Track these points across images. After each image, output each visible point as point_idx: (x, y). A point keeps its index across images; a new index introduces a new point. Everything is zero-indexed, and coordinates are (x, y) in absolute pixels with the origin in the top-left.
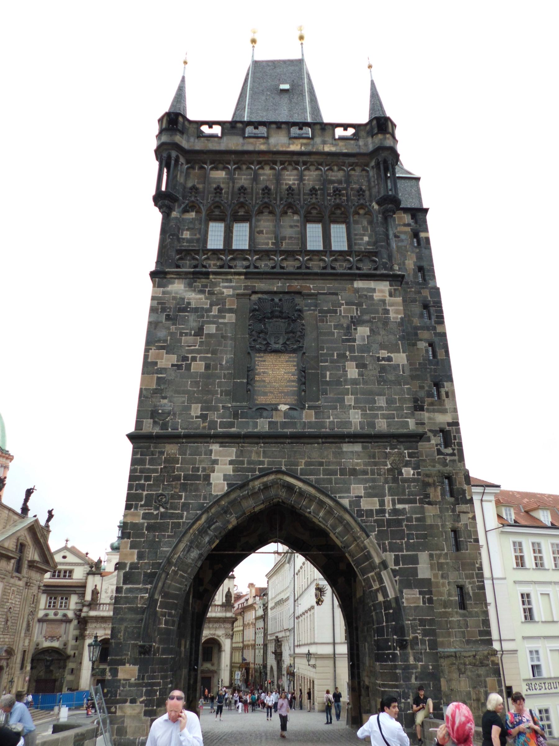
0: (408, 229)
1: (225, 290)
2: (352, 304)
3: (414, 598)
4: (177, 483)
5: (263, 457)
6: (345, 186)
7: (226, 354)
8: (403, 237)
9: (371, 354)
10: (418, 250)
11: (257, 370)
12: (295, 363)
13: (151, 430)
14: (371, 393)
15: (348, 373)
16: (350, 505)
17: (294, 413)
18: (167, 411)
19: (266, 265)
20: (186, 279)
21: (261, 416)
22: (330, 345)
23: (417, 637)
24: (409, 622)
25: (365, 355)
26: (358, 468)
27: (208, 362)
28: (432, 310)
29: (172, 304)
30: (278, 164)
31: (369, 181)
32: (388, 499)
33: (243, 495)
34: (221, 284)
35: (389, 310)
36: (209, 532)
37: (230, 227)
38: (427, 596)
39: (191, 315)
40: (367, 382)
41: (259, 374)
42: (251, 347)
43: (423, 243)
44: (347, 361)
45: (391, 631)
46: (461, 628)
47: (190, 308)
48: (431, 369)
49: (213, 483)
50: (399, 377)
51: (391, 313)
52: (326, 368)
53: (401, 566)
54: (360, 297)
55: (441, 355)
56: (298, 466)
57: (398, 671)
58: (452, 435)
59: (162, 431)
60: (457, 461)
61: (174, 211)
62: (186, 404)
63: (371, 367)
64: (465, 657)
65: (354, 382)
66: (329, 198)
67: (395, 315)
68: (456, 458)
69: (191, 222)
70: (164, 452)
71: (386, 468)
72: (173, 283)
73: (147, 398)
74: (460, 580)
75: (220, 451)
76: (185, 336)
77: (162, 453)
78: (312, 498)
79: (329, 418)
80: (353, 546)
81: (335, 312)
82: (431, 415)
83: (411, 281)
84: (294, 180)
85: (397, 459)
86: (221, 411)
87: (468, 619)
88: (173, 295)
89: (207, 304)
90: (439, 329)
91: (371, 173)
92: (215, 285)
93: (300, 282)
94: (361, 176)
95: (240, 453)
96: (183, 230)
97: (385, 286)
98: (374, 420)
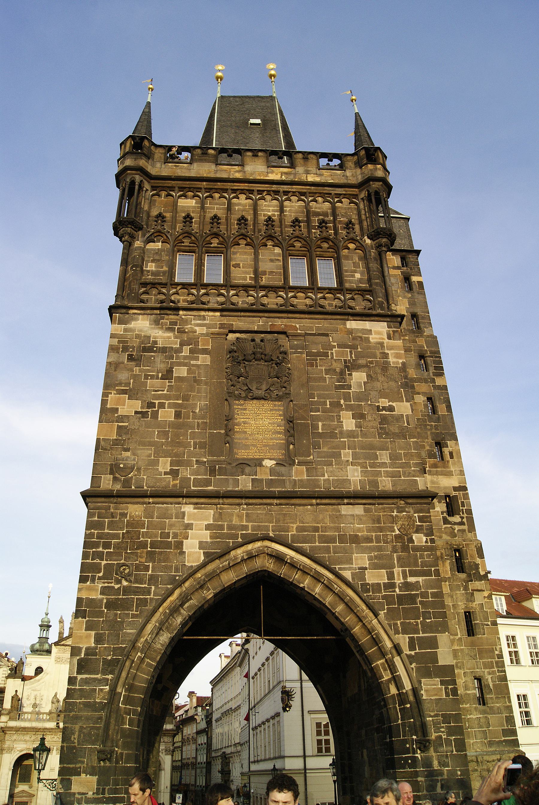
0: (398, 272)
1: (197, 328)
2: (346, 346)
3: (434, 688)
4: (143, 551)
5: (247, 522)
6: (332, 218)
7: (199, 401)
9: (369, 403)
10: (410, 295)
11: (236, 419)
12: (281, 413)
14: (372, 447)
16: (353, 579)
17: (282, 469)
19: (244, 302)
21: (243, 473)
22: (322, 392)
23: (440, 737)
24: (431, 719)
25: (363, 403)
26: (360, 534)
27: (178, 410)
28: (429, 360)
29: (136, 343)
30: (255, 193)
32: (397, 570)
33: (223, 567)
34: (193, 322)
36: (182, 611)
37: (201, 260)
38: (450, 687)
39: (158, 356)
40: (366, 434)
41: (238, 424)
42: (229, 393)
43: (415, 287)
45: (410, 731)
46: (481, 727)
47: (156, 347)
49: (187, 551)
51: (390, 357)
52: (318, 418)
53: (417, 651)
54: (354, 339)
55: (442, 409)
56: (288, 532)
57: (419, 779)
58: (460, 501)
59: (124, 489)
60: (467, 531)
62: (153, 458)
63: (370, 418)
64: (488, 762)
65: (351, 434)
66: (314, 231)
67: (395, 360)
68: (465, 527)
69: (157, 253)
70: (127, 514)
71: (394, 534)
74: (478, 670)
75: (195, 514)
76: (150, 379)
77: (124, 515)
78: (305, 572)
80: (357, 628)
82: (435, 478)
83: (404, 329)
84: (273, 211)
85: (406, 523)
86: (195, 466)
87: (489, 716)
89: (176, 344)
91: (362, 206)
94: (349, 208)
95: (219, 516)
96: (148, 262)
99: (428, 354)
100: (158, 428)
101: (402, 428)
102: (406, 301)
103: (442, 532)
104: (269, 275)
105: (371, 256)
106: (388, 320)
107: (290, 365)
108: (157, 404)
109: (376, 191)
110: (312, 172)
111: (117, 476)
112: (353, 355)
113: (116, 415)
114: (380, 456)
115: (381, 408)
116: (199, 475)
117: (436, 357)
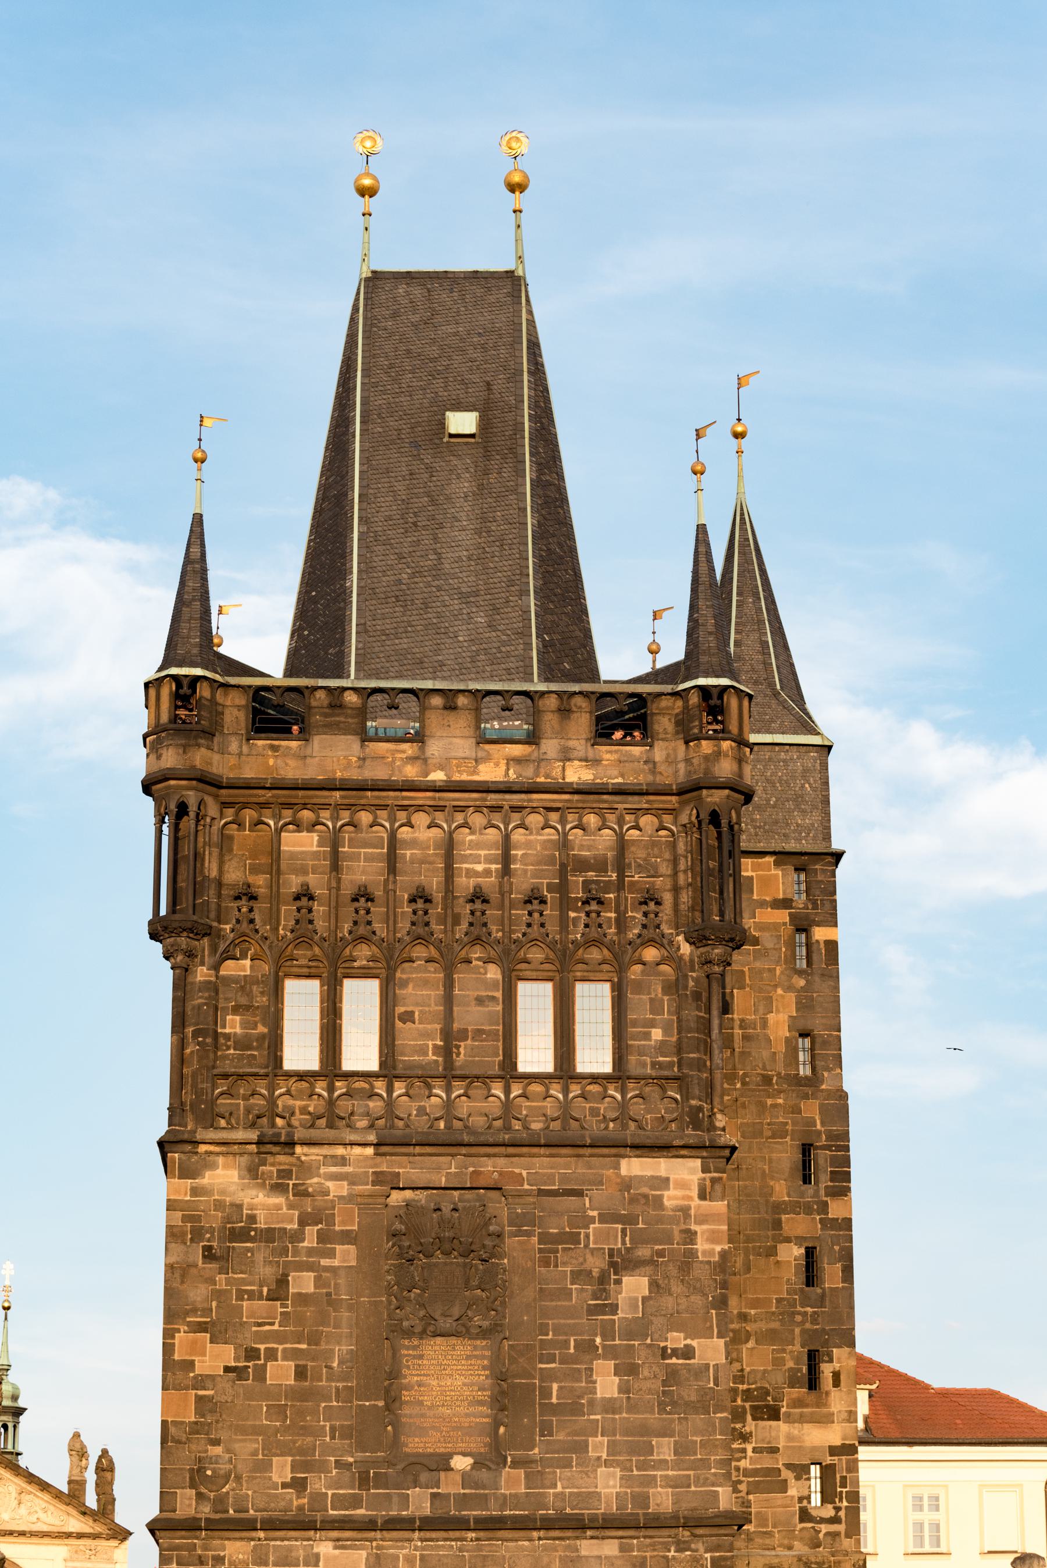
0: (782, 916)
1: (330, 1184)
2: (615, 1218)
7: (339, 1344)
8: (767, 940)
9: (649, 1341)
10: (802, 983)
11: (405, 1377)
13: (192, 1512)
14: (645, 1430)
15: (598, 1385)
17: (484, 1475)
18: (222, 1472)
19: (422, 1111)
20: (241, 1154)
21: (416, 1484)
22: (562, 1321)
25: (636, 1343)
27: (300, 1363)
28: (822, 1157)
29: (214, 1220)
31: (675, 862)
34: (322, 1171)
35: (696, 1233)
39: (259, 1248)
42: (391, 1325)
44: (598, 1357)
47: (255, 1229)
48: (806, 1313)
50: (706, 1394)
51: (699, 1240)
54: (633, 1200)
55: (831, 1275)
58: (838, 1476)
61: (202, 964)
62: (260, 1457)
63: (646, 1373)
65: (610, 1406)
66: (572, 914)
67: (707, 1246)
72: (213, 1166)
73: (179, 1442)
75: (336, 1557)
76: (248, 1299)
79: (555, 1486)
81: (574, 1238)
82: (795, 1429)
83: (779, 1074)
84: (489, 860)
86: (334, 1471)
88: (216, 1197)
89: (291, 1221)
90: (835, 1210)
92: (306, 1169)
93: (501, 1161)
94: (654, 844)
97: (692, 1171)
98: (645, 1490)
99: (823, 1141)
100: (268, 1400)
101: (703, 1392)
102: (792, 997)
103: (794, 1538)
104: (473, 1039)
105: (686, 988)
106: (705, 1154)
107: (506, 1261)
108: (262, 1352)
109: (714, 810)
110: (575, 754)
111: (203, 1490)
112: (627, 1239)
113: (192, 1375)
114: (658, 1448)
115: (669, 1351)
116: (341, 1488)
117: (839, 1148)
